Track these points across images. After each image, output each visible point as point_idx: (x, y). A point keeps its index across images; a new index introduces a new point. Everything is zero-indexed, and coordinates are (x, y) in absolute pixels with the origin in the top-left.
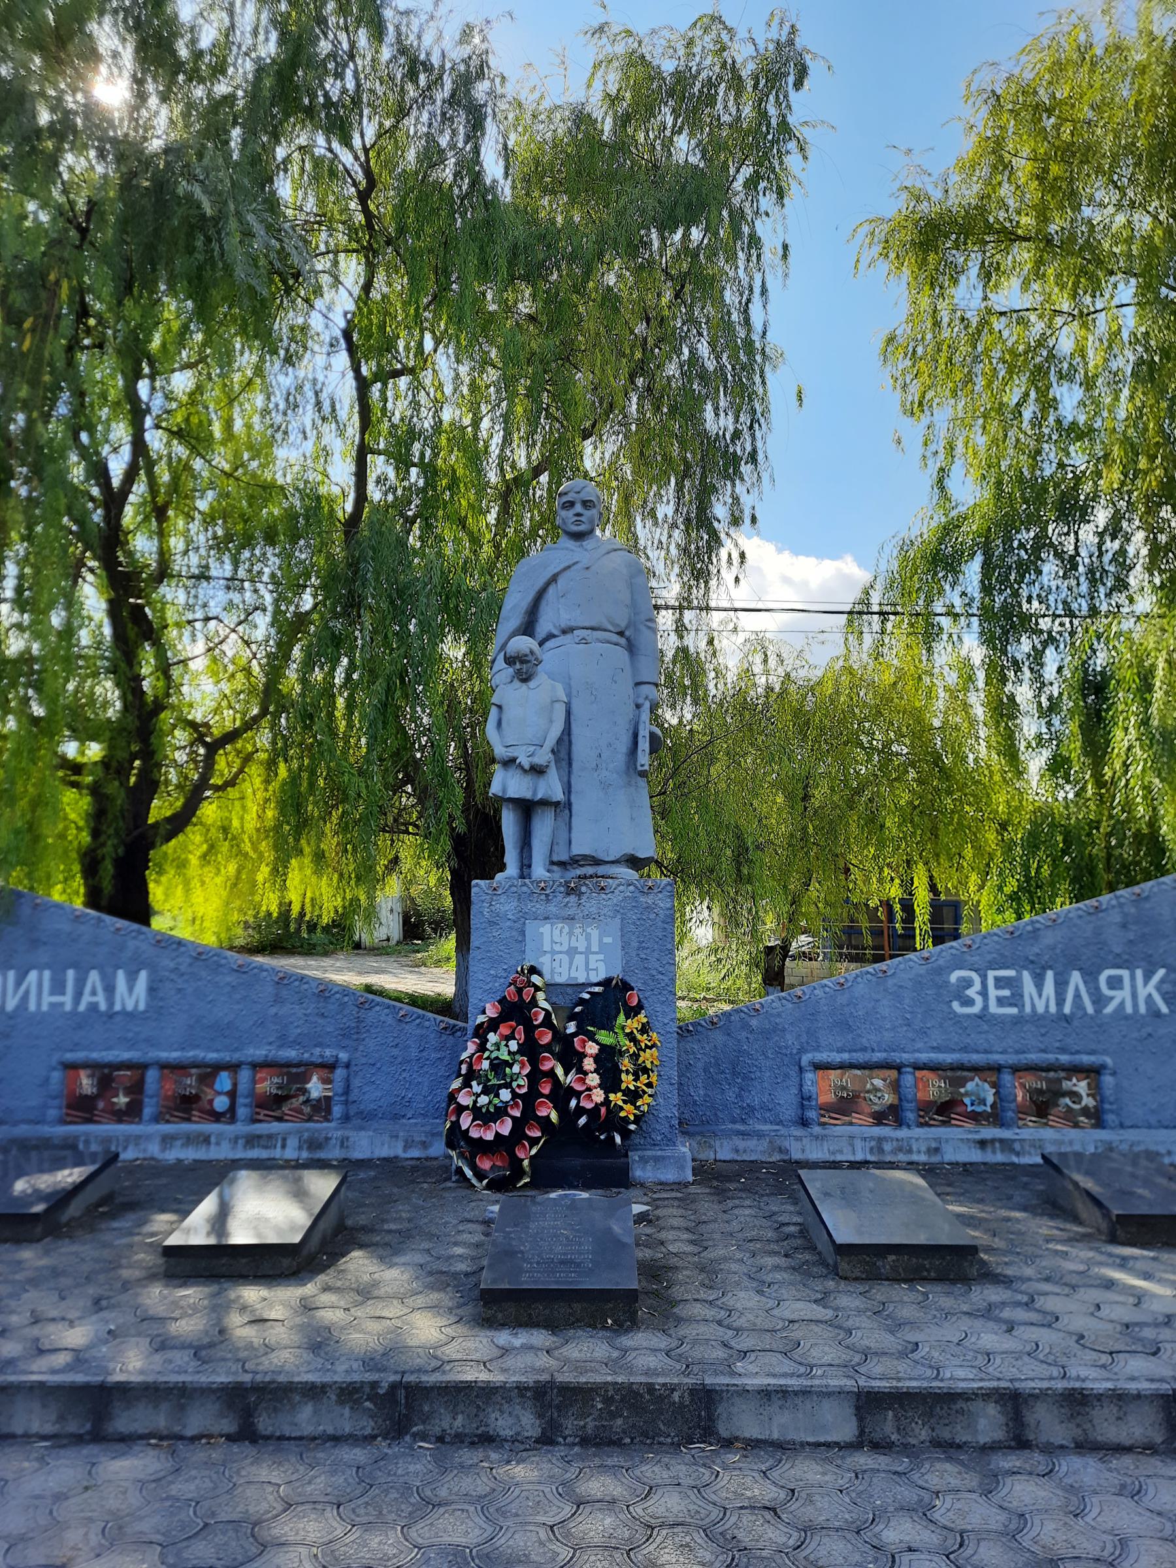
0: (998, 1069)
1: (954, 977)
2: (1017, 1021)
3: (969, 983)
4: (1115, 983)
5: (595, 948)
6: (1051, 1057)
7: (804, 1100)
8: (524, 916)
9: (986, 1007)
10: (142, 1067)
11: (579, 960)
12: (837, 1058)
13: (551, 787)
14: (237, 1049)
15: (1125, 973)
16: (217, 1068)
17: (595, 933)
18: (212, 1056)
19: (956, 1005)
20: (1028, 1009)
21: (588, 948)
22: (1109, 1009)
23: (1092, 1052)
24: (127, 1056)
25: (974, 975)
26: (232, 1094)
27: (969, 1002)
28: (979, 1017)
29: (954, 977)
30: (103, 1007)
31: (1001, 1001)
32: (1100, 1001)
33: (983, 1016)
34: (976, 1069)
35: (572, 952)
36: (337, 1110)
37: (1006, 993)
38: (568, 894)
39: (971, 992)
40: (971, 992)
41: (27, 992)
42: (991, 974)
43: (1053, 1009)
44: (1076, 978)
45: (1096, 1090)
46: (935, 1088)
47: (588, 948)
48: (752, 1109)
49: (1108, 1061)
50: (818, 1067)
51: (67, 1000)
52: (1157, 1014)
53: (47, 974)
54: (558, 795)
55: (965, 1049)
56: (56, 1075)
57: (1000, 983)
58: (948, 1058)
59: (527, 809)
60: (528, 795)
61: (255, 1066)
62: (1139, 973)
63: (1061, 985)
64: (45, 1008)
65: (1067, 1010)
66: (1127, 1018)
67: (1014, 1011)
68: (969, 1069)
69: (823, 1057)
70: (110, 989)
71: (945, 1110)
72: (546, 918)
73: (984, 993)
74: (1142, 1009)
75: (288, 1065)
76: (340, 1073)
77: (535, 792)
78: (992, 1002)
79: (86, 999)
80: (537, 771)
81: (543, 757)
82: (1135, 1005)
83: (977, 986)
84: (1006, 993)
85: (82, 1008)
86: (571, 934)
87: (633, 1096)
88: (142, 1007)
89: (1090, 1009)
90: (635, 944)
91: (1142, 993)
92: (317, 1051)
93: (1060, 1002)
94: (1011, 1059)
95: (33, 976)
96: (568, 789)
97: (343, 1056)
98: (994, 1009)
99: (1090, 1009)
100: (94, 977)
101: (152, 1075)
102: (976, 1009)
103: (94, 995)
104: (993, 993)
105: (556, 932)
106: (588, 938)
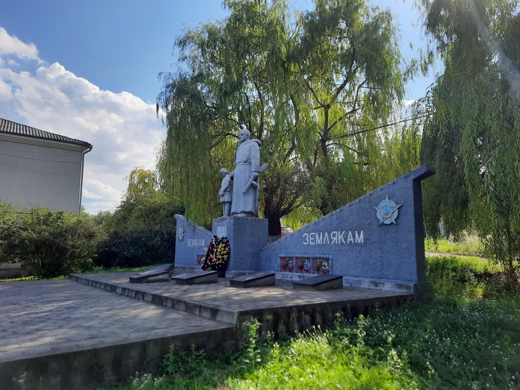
2: (315, 246)
3: (306, 237)
4: (334, 235)
6: (319, 255)
8: (218, 225)
9: (309, 242)
15: (336, 232)
22: (332, 243)
27: (306, 242)
28: (308, 245)
32: (331, 240)
33: (308, 245)
37: (313, 239)
39: (307, 239)
40: (307, 239)
42: (311, 234)
46: (300, 263)
48: (271, 268)
49: (331, 257)
52: (342, 244)
55: (305, 253)
56: (196, 257)
58: (301, 255)
63: (323, 236)
66: (336, 245)
67: (314, 243)
68: (306, 258)
69: (281, 255)
73: (309, 239)
82: (338, 241)
83: (308, 237)
84: (313, 239)
87: (219, 259)
91: (339, 238)
93: (323, 241)
98: (311, 243)
102: (307, 243)
104: (311, 239)
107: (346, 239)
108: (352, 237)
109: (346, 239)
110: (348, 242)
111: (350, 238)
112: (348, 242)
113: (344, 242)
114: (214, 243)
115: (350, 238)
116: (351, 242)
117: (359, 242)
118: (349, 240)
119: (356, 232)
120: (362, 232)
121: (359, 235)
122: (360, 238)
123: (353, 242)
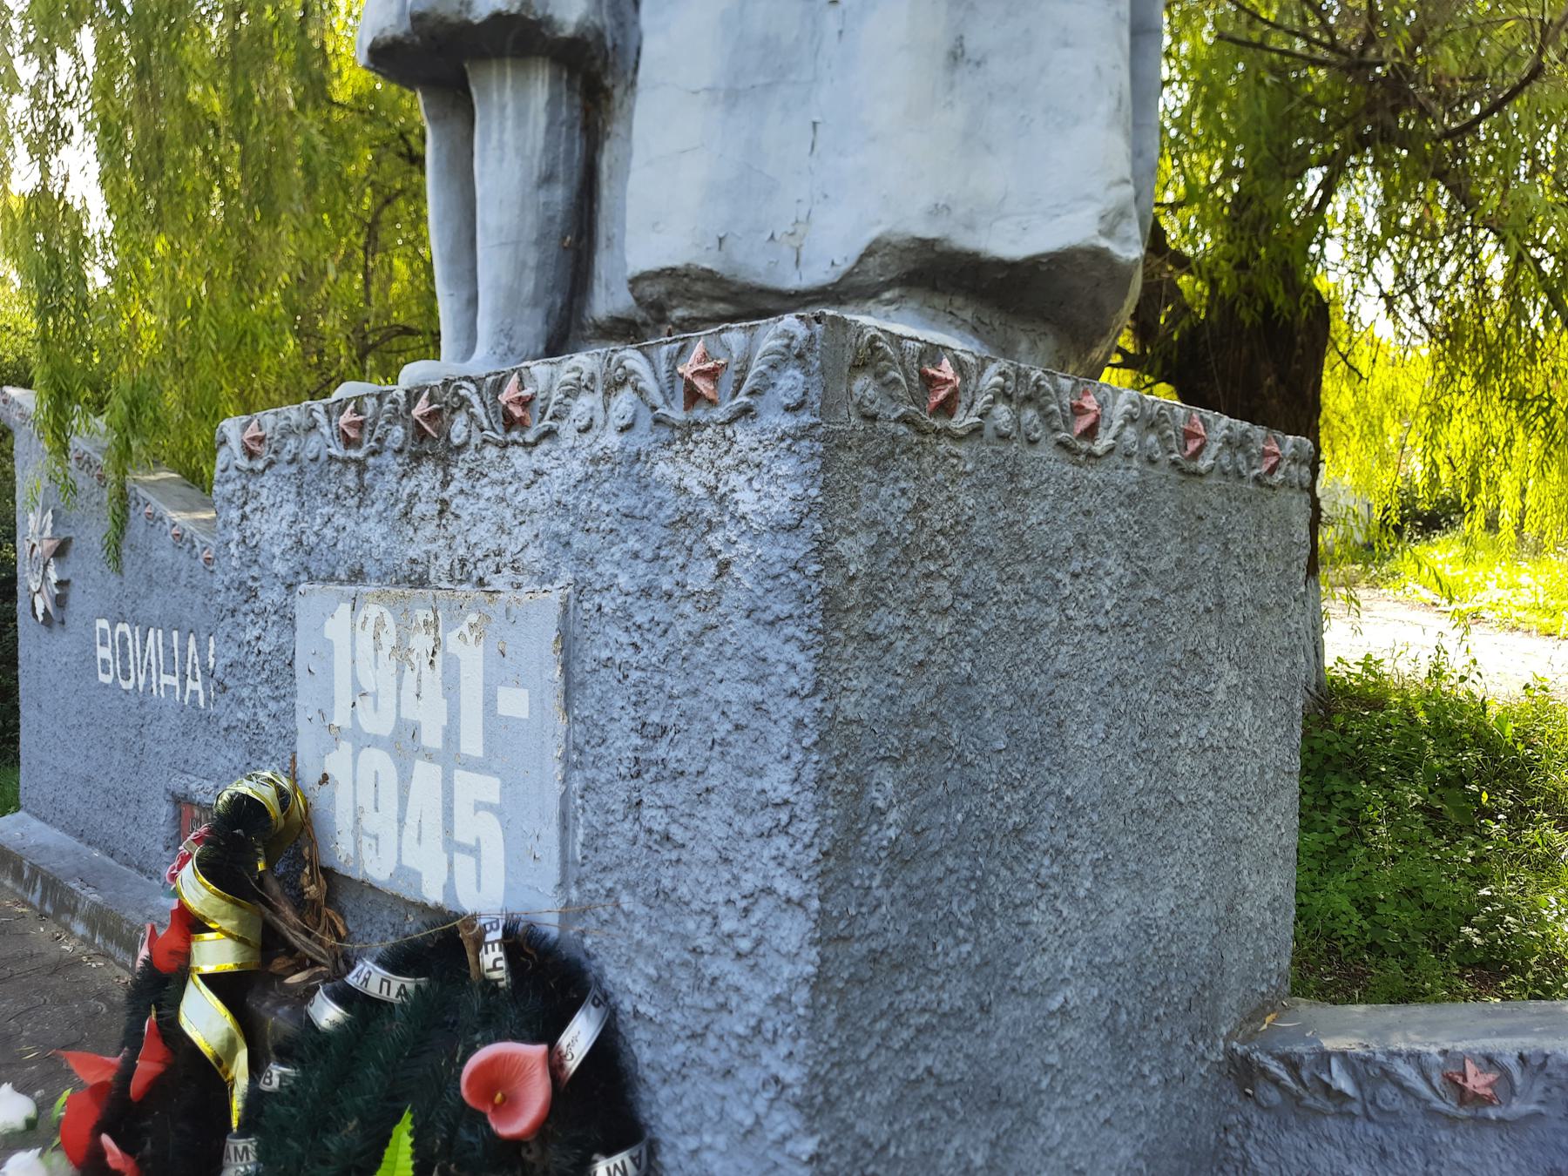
5: (472, 743)
8: (315, 565)
17: (470, 656)
21: (451, 734)
38: (417, 458)
47: (451, 734)
51: (174, 681)
72: (357, 575)
79: (190, 684)
86: (402, 651)
90: (623, 742)
105: (365, 641)
114: (204, 1020)
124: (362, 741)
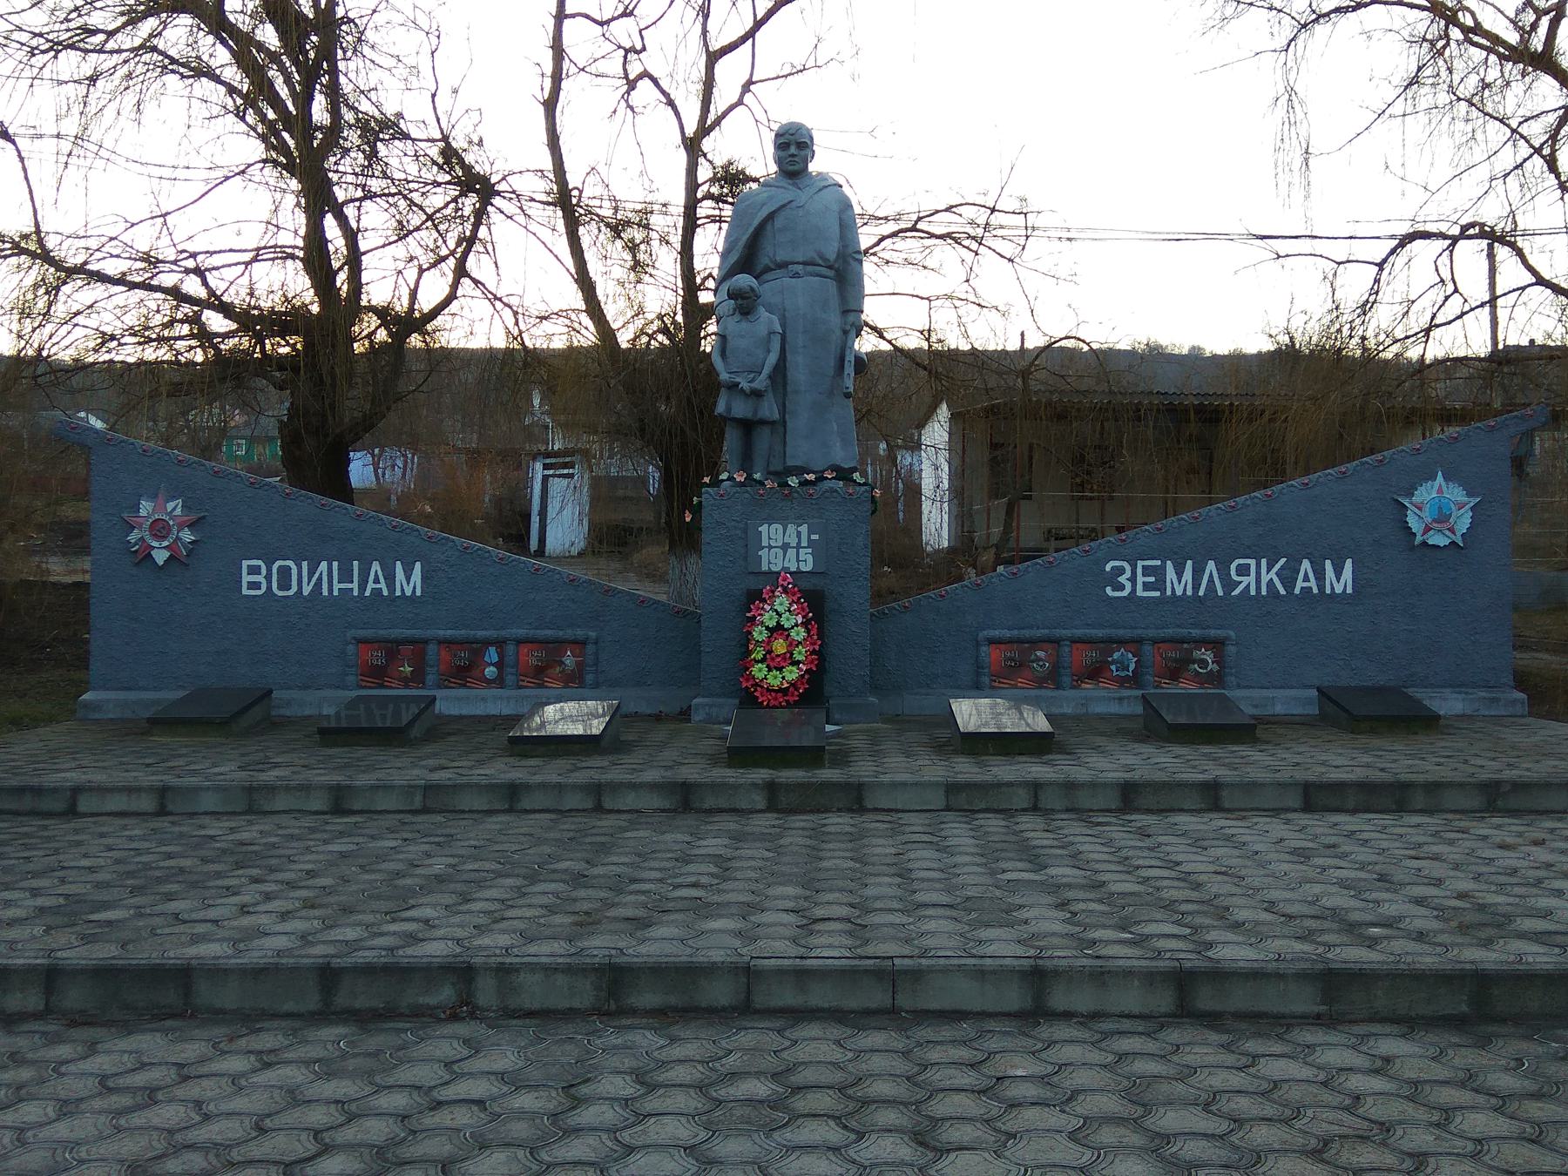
0: (1139, 641)
1: (1108, 568)
2: (1162, 600)
3: (1121, 571)
5: (804, 544)
7: (978, 667)
9: (1134, 590)
10: (426, 642)
11: (791, 553)
12: (1007, 634)
13: (769, 409)
14: (502, 628)
15: (1252, 562)
16: (487, 643)
18: (481, 634)
19: (1109, 590)
20: (1169, 592)
22: (1236, 592)
23: (1221, 627)
24: (408, 633)
25: (1125, 564)
26: (499, 665)
27: (1122, 588)
29: (1108, 568)
30: (385, 593)
31: (1146, 586)
32: (1229, 585)
34: (1121, 642)
35: (785, 547)
36: (589, 678)
37: (1152, 579)
39: (1122, 579)
40: (1122, 579)
41: (320, 579)
42: (1140, 564)
43: (1189, 592)
44: (1211, 565)
45: (1219, 660)
46: (1089, 656)
49: (1232, 633)
50: (992, 642)
51: (355, 586)
53: (335, 564)
54: (776, 416)
57: (1147, 571)
58: (1099, 633)
59: (748, 427)
60: (749, 416)
61: (519, 642)
62: (1264, 562)
64: (336, 593)
65: (1201, 593)
67: (1157, 594)
70: (390, 578)
71: (1095, 672)
73: (1133, 580)
74: (1264, 592)
75: (547, 642)
76: (590, 648)
77: (755, 412)
78: (1139, 587)
79: (371, 585)
80: (757, 394)
81: (761, 382)
83: (1128, 574)
84: (1152, 579)
85: (367, 593)
88: (418, 593)
89: (1220, 593)
91: (1265, 579)
92: (569, 631)
93: (1196, 587)
94: (1151, 633)
95: (324, 565)
96: (783, 410)
97: (593, 634)
98: (1140, 592)
99: (1220, 593)
100: (376, 566)
101: (432, 649)
103: (376, 581)
104: (1140, 579)
106: (799, 534)
107: (1289, 582)
108: (1311, 575)
109: (1289, 582)
110: (1297, 591)
111: (1306, 579)
112: (1297, 591)
113: (1282, 592)
115: (1306, 579)
116: (1307, 591)
117: (1339, 589)
118: (1300, 584)
119: (1328, 563)
120: (1349, 563)
121: (1338, 574)
122: (1342, 581)
123: (1315, 591)
124: (770, 547)
